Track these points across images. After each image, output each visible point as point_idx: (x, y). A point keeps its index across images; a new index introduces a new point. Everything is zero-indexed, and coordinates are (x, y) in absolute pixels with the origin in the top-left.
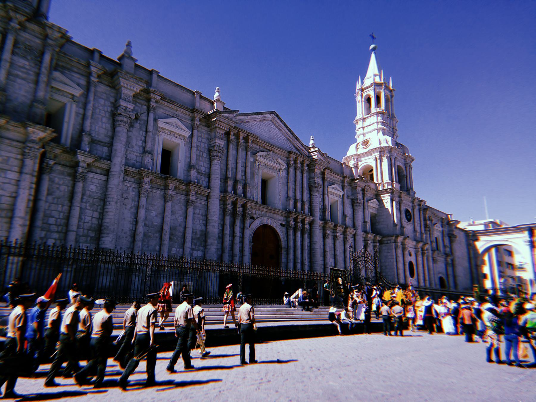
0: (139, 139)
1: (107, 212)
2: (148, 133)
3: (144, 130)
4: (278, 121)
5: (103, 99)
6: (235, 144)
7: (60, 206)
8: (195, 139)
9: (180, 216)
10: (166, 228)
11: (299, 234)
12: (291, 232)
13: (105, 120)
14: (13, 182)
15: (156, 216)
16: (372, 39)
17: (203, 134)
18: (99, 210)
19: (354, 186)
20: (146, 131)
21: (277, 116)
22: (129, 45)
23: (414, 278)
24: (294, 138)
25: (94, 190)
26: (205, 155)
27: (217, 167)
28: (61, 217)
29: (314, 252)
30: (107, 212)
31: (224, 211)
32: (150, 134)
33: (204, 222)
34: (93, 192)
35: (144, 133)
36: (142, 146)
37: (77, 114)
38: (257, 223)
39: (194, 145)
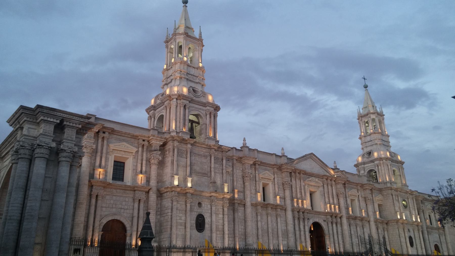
0: (253, 185)
1: (248, 226)
3: (255, 180)
4: (315, 157)
5: (238, 170)
6: (294, 177)
7: (230, 225)
8: (276, 180)
9: (275, 223)
10: (270, 230)
11: (334, 225)
12: (330, 225)
14: (221, 219)
15: (265, 224)
16: (365, 77)
17: (279, 176)
18: (243, 225)
19: (365, 188)
20: (256, 181)
21: (314, 155)
22: (244, 140)
23: (414, 247)
24: (325, 166)
25: (240, 215)
28: (231, 230)
29: (345, 236)
30: (248, 226)
31: (294, 218)
32: (257, 182)
33: (285, 225)
34: (240, 216)
35: (255, 182)
36: (255, 189)
37: (230, 179)
38: (311, 222)
39: (276, 183)
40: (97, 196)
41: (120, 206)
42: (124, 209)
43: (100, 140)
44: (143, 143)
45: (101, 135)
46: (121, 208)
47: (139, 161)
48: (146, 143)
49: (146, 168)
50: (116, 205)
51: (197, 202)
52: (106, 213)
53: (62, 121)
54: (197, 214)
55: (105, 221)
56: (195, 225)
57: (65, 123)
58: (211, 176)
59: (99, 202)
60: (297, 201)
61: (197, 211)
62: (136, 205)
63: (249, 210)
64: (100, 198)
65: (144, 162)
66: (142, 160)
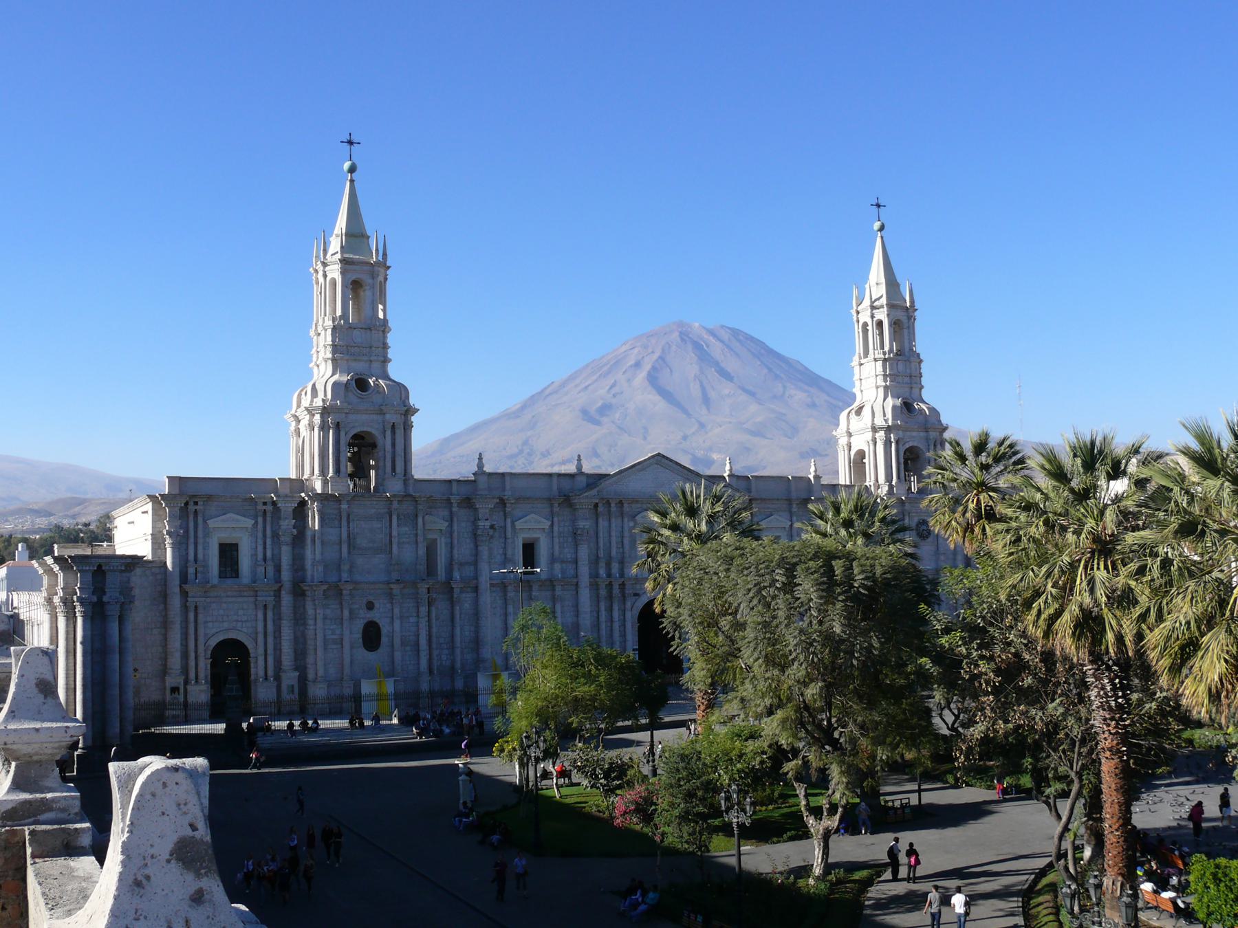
2: (508, 540)
3: (503, 536)
8: (556, 528)
13: (468, 541)
20: (505, 538)
21: (664, 456)
26: (570, 539)
27: (584, 552)
32: (509, 541)
39: (556, 534)
40: (196, 607)
41: (235, 618)
42: (241, 621)
43: (191, 518)
44: (264, 507)
45: (191, 508)
46: (237, 621)
47: (260, 542)
48: (269, 508)
49: (273, 549)
50: (228, 616)
51: (365, 601)
52: (215, 630)
53: (100, 566)
54: (365, 621)
55: (213, 642)
56: (361, 640)
57: (104, 568)
58: (391, 552)
59: (200, 617)
60: (608, 565)
61: (365, 616)
62: (260, 615)
63: (488, 598)
64: (200, 610)
65: (269, 541)
66: (265, 536)
